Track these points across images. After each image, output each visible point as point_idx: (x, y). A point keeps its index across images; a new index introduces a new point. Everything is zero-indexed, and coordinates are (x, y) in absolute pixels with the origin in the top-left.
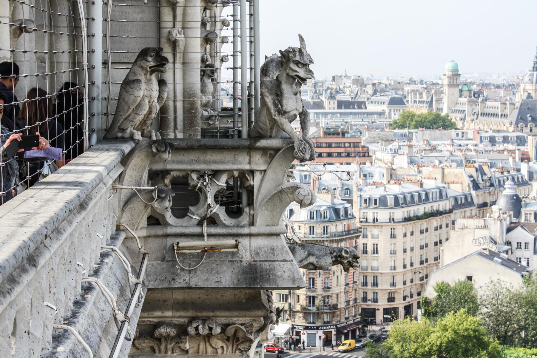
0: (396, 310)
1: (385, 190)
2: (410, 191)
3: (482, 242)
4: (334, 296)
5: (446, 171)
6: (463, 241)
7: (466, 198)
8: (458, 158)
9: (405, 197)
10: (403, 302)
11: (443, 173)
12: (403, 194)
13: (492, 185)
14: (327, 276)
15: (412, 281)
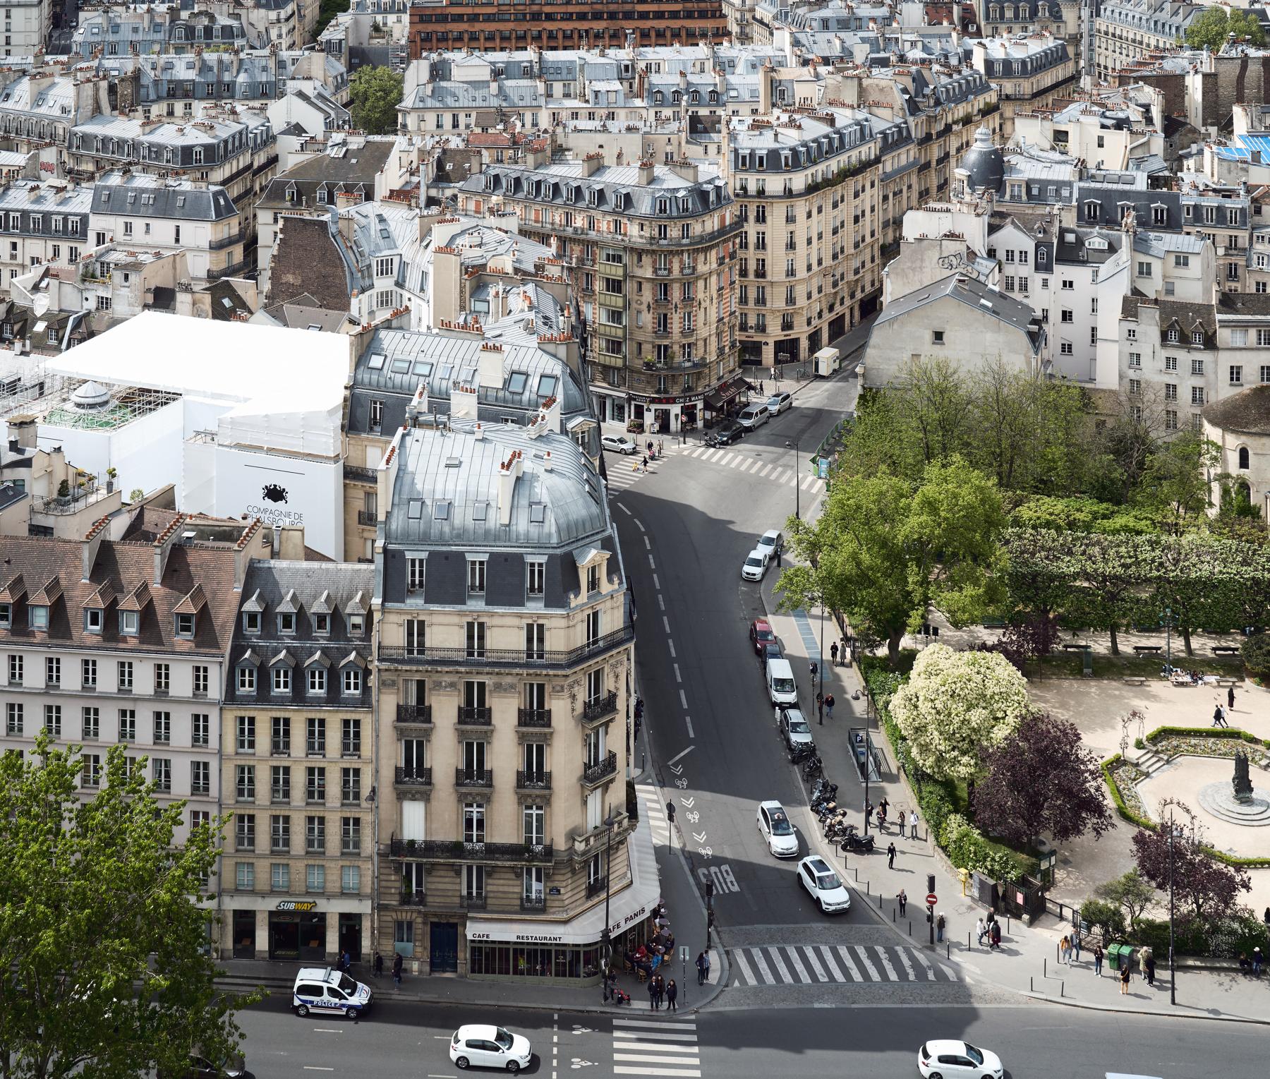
0: (795, 342)
1: (776, 140)
2: (815, 136)
3: (955, 263)
4: (700, 343)
5: (865, 82)
6: (922, 260)
7: (900, 132)
8: (871, 34)
9: (808, 151)
10: (806, 328)
11: (860, 85)
12: (805, 145)
13: (938, 103)
14: (688, 310)
15: (820, 291)
